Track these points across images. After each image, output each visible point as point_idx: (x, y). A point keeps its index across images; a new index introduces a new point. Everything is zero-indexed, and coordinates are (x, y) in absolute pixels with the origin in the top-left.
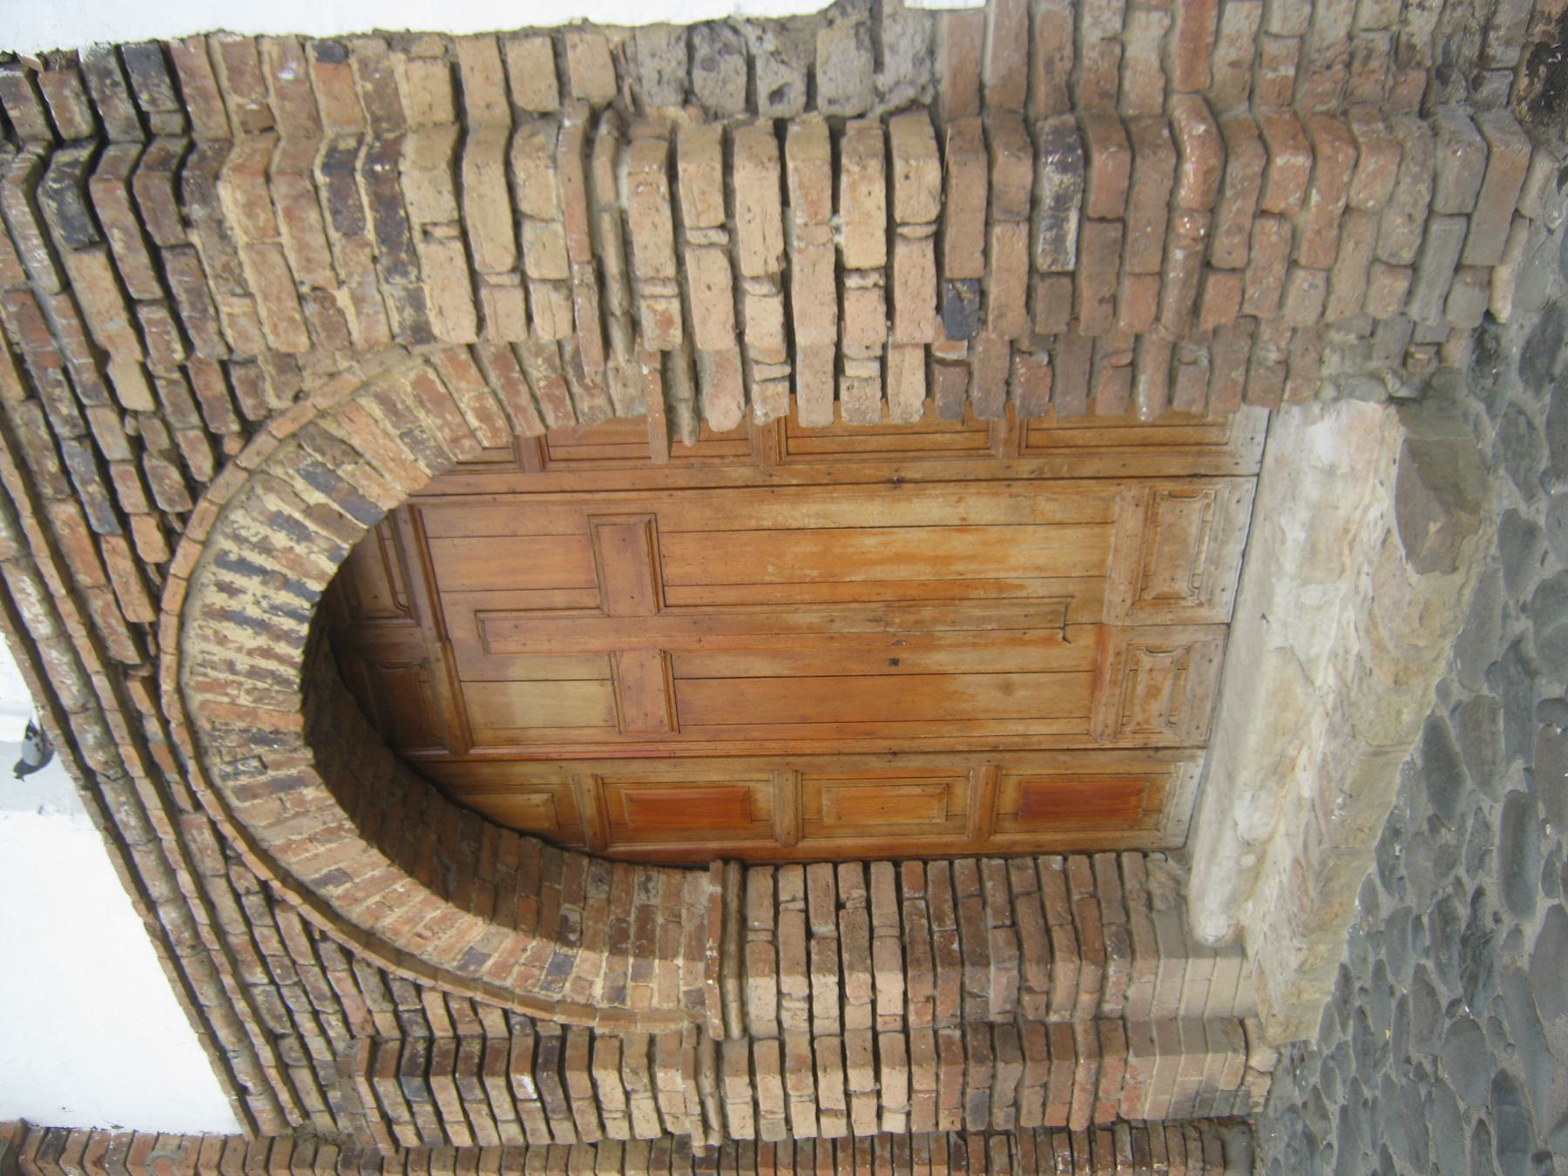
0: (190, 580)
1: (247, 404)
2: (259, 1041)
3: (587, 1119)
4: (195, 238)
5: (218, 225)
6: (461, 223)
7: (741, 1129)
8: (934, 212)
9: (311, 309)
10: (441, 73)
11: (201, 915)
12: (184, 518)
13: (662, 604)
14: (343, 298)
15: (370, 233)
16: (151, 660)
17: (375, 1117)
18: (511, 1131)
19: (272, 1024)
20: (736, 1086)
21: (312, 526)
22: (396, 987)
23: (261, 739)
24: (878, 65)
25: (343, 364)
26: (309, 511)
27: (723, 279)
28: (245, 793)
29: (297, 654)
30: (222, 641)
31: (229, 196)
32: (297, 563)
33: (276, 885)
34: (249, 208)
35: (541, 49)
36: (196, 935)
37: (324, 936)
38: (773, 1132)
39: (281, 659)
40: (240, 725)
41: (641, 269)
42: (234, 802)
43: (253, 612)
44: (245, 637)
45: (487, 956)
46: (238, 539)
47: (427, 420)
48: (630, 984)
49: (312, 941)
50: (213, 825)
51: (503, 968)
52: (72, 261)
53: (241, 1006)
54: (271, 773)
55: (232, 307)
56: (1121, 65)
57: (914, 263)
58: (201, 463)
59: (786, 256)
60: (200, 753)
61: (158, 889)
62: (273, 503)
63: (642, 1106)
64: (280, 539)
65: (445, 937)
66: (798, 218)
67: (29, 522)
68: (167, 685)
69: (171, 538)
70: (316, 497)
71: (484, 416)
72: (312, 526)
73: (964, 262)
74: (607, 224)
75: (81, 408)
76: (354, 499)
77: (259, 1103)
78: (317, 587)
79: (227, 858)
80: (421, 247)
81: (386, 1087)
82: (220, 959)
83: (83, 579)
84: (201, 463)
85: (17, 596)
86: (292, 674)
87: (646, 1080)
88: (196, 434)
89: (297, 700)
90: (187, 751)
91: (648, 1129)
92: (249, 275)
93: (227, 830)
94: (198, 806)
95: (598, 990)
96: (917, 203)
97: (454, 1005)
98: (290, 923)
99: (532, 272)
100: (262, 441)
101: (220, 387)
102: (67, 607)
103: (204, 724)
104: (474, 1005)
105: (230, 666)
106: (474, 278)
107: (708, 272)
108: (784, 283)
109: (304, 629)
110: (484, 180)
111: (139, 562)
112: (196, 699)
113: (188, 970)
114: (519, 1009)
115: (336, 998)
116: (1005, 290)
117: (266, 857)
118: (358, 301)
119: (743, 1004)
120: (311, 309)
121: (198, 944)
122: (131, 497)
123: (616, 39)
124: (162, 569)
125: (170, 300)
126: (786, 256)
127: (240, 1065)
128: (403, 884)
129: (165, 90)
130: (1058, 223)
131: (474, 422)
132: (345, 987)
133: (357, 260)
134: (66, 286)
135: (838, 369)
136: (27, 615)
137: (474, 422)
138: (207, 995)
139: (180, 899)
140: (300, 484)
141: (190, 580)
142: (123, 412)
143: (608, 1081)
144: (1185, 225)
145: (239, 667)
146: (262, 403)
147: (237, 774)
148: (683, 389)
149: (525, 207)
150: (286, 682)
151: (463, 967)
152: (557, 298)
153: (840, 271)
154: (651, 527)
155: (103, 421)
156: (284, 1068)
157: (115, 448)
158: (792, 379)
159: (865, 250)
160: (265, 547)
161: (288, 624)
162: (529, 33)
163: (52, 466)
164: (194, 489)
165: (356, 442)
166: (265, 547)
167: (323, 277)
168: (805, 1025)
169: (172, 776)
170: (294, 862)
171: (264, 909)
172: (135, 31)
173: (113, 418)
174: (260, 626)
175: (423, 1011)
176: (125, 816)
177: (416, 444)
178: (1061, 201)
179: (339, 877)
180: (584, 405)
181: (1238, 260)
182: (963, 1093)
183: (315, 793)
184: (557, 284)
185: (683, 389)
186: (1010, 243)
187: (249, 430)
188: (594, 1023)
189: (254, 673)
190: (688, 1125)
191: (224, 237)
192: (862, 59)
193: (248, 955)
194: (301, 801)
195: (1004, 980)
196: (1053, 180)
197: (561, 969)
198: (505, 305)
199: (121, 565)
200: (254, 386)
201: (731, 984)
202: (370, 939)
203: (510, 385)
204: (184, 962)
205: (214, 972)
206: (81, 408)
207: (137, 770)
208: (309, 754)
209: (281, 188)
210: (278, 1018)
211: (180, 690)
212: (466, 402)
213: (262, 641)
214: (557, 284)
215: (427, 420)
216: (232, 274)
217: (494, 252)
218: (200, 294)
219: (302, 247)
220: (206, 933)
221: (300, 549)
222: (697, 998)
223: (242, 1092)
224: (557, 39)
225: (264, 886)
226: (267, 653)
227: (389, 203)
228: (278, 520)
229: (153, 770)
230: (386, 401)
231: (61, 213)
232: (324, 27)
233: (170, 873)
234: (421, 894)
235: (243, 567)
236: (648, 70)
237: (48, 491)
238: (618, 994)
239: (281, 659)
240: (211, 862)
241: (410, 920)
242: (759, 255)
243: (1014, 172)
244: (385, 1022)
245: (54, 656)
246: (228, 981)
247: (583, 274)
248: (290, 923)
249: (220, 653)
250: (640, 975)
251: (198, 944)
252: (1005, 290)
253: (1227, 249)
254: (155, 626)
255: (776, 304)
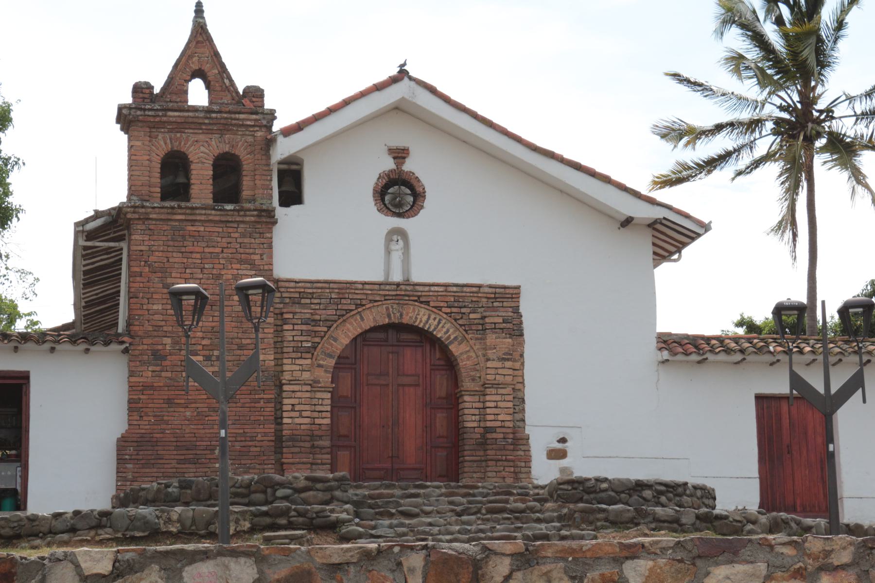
0: (439, 314)
1: (471, 332)
2: (315, 291)
3: (294, 355)
4: (504, 334)
5: (506, 338)
6: (504, 368)
7: (285, 388)
8: (506, 426)
9: (493, 347)
10: (519, 368)
11: (357, 292)
12: (450, 317)
13: (399, 385)
14: (495, 351)
15: (503, 356)
16: (421, 302)
17: (298, 310)
18: (291, 339)
19: (317, 294)
20: (308, 388)
21: (447, 335)
22: (331, 323)
23: (401, 315)
24: (517, 421)
25: (477, 347)
26: (450, 335)
27: (497, 400)
28: (387, 309)
29: (421, 326)
30: (424, 315)
31: (510, 340)
32: (439, 331)
33: (364, 308)
34: (509, 342)
35: (521, 381)
36: (352, 289)
37: (347, 313)
38: (284, 395)
39: (419, 323)
40: (404, 313)
41: (499, 390)
42: (384, 306)
43: (430, 322)
44: (425, 319)
45: (336, 342)
46: (445, 323)
47: (465, 356)
48: (323, 369)
49: (346, 310)
50: (382, 301)
51: (332, 345)
52: (501, 318)
53: (328, 291)
54: (392, 315)
55: (494, 336)
56: (518, 450)
57: (499, 424)
58: (461, 322)
59: (500, 408)
60: (397, 304)
61: (367, 287)
62: (451, 330)
63: (297, 368)
64: (445, 330)
65: (343, 336)
66: (506, 410)
67: (453, 294)
68: (416, 303)
69: (446, 313)
70: (452, 337)
71: (465, 364)
72: (447, 335)
73: (498, 430)
74: (506, 386)
75: (470, 308)
76: (451, 342)
77: (292, 284)
78: (435, 333)
79: (370, 300)
80: (501, 362)
81: (308, 316)
82: (344, 291)
83: (439, 298)
84: (461, 322)
85: (439, 287)
86: (416, 324)
87: (307, 369)
88: (466, 323)
89: (410, 323)
90: (401, 302)
91: (286, 368)
92: (498, 340)
93: (380, 303)
94: (385, 300)
95: (321, 362)
96: (507, 424)
97: (322, 333)
98: (353, 307)
99: (497, 376)
100: (464, 333)
101: (473, 329)
102: (436, 294)
103: (405, 306)
104: (322, 338)
105: (419, 315)
106: (496, 368)
107: (498, 398)
108: (496, 407)
109: (426, 329)
110: (510, 372)
111: (441, 307)
112: (412, 307)
113: (342, 284)
114: (320, 346)
115: (325, 309)
116: (494, 435)
117: (368, 308)
118: (494, 353)
119: (325, 391)
120: (493, 347)
121: (348, 288)
122: (454, 310)
123: (523, 390)
124: (441, 310)
125: (495, 328)
126: (500, 408)
127: (309, 285)
128: (360, 331)
129: (517, 334)
130: (504, 442)
131: (464, 363)
132: (329, 312)
133: (500, 354)
134: (498, 316)
135: (473, 415)
136: (436, 287)
137: (464, 363)
138: (335, 286)
139: (362, 289)
140: (455, 335)
141: (439, 314)
142: (469, 313)
143: (309, 361)
144: (504, 457)
145: (418, 316)
146: (470, 334)
147: (393, 309)
148: (472, 393)
149: (506, 376)
150: (415, 322)
151: (332, 336)
152: (493, 378)
153: (497, 414)
154: (418, 385)
155: (468, 310)
156: (300, 293)
157: (463, 310)
158: (472, 408)
159: (500, 417)
160: (443, 327)
161: (427, 326)
162: (524, 380)
163: (461, 300)
164: (456, 320)
165: (462, 345)
166: (443, 327)
167: (498, 349)
168: (313, 403)
169: (394, 298)
170: (368, 312)
171: (356, 303)
172: (525, 332)
173: (469, 312)
174: (427, 322)
175: (320, 326)
176: (388, 287)
177: (461, 354)
178: (507, 442)
179: (362, 319)
180: (467, 379)
181: (498, 465)
182: (299, 435)
183: (387, 321)
184: (495, 379)
185: (472, 393)
186: (501, 436)
187: (465, 330)
188: (314, 360)
189: (416, 318)
190: (286, 376)
191: (504, 338)
192: (518, 419)
193: (341, 296)
194: (385, 318)
195: (326, 444)
196: (510, 441)
197: (330, 356)
198: (493, 371)
199: (442, 304)
200: (474, 333)
201: (331, 390)
202: (344, 321)
203: (471, 369)
204: (345, 285)
205: (339, 289)
206: (470, 308)
207: (398, 293)
208: (397, 322)
209: (511, 347)
210: (319, 296)
211: (415, 305)
212: (468, 362)
213: (424, 321)
214: (495, 379)
215: (465, 356)
216: (499, 338)
217: (500, 371)
218: (496, 333)
219: (502, 348)
220: (353, 291)
221: (443, 332)
222: (319, 382)
223: (296, 282)
224: (523, 383)
225: (364, 305)
226: (421, 321)
227: (508, 360)
228: (448, 331)
229: (397, 295)
230: (469, 351)
231: (508, 319)
232: (525, 355)
233: (371, 290)
234: (357, 333)
235: (439, 323)
236: (518, 393)
237: (456, 298)
238: (320, 366)
239: (419, 323)
240: (370, 298)
241: (348, 329)
242: (500, 404)
243: (511, 436)
244: (317, 317)
245: (427, 288)
246: (337, 291)
247: (496, 382)
248: (353, 307)
249: (421, 314)
250: (326, 371)
251: (348, 288)
252: (494, 435)
253: (500, 463)
254: (429, 305)
255: (493, 406)
